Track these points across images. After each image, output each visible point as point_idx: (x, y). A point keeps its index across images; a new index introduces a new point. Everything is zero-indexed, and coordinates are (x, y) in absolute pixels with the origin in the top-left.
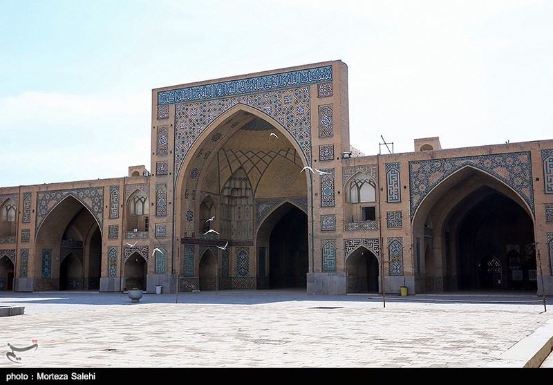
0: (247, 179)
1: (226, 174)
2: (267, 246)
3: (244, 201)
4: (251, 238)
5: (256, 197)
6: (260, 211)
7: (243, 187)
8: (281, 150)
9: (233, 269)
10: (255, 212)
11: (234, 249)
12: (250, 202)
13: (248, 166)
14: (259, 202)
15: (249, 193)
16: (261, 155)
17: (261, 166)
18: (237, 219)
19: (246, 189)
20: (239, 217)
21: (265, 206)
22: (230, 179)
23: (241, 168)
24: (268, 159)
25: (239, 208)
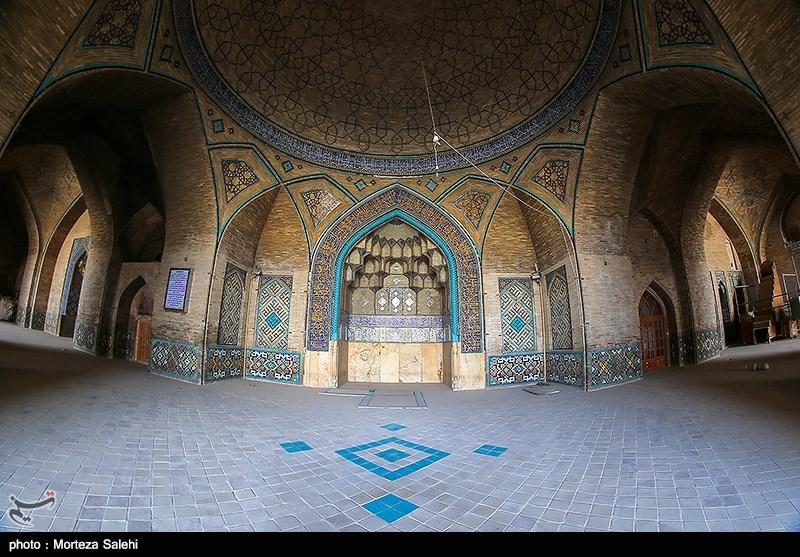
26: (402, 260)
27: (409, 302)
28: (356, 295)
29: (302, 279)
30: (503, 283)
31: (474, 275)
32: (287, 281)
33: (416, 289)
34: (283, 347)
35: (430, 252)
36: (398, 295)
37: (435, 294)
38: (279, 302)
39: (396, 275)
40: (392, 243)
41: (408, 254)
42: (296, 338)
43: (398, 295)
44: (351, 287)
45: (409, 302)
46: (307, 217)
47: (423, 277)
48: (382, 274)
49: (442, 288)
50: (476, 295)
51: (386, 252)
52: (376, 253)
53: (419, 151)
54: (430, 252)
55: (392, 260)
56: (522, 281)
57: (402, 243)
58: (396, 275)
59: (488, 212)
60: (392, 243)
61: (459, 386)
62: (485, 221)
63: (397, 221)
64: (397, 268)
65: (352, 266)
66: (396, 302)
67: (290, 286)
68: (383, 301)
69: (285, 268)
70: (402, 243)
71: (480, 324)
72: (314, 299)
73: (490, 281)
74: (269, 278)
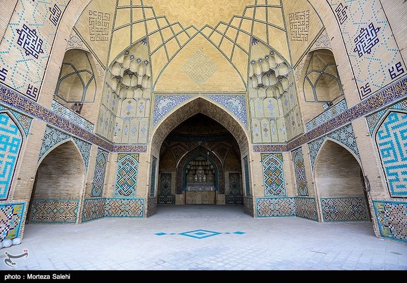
0: (148, 63)
1: (122, 41)
2: (158, 157)
3: (138, 93)
4: (143, 140)
5: (155, 88)
6: (160, 107)
7: (141, 73)
8: (207, 26)
9: (110, 186)
10: (153, 108)
11: (113, 156)
12: (147, 94)
13: (155, 41)
14: (159, 96)
15: (146, 84)
16: (177, 29)
17: (172, 46)
18: (124, 115)
19: (145, 76)
20: (128, 113)
21: (168, 101)
22: (126, 52)
23: (144, 40)
24: (183, 38)
25: (130, 102)
26: (202, 166)
27: (204, 178)
28: (188, 176)
29: (174, 175)
30: (230, 175)
31: (222, 172)
32: (170, 175)
33: (206, 174)
34: (169, 194)
35: (210, 165)
36: (201, 176)
37: (212, 176)
38: (167, 181)
39: (200, 171)
40: (199, 161)
41: (204, 164)
42: (173, 191)
43: (201, 176)
44: (187, 174)
45: (204, 178)
46: (174, 156)
47: (209, 170)
48: (196, 170)
49: (214, 174)
50: (223, 178)
51: (197, 163)
52: (194, 164)
53: (207, 133)
54: (210, 165)
55: (199, 166)
56: (236, 174)
57: (202, 161)
58: (200, 171)
59: (226, 154)
60: (199, 161)
61: (218, 203)
62: (225, 157)
63: (200, 156)
64: (200, 168)
65: (187, 169)
66: (200, 178)
67: (171, 176)
68: (196, 178)
69: (169, 171)
70: (202, 161)
71: (223, 186)
72: (178, 179)
73: (227, 174)
74: (164, 174)
